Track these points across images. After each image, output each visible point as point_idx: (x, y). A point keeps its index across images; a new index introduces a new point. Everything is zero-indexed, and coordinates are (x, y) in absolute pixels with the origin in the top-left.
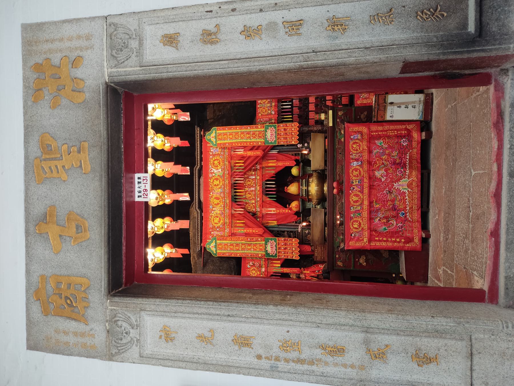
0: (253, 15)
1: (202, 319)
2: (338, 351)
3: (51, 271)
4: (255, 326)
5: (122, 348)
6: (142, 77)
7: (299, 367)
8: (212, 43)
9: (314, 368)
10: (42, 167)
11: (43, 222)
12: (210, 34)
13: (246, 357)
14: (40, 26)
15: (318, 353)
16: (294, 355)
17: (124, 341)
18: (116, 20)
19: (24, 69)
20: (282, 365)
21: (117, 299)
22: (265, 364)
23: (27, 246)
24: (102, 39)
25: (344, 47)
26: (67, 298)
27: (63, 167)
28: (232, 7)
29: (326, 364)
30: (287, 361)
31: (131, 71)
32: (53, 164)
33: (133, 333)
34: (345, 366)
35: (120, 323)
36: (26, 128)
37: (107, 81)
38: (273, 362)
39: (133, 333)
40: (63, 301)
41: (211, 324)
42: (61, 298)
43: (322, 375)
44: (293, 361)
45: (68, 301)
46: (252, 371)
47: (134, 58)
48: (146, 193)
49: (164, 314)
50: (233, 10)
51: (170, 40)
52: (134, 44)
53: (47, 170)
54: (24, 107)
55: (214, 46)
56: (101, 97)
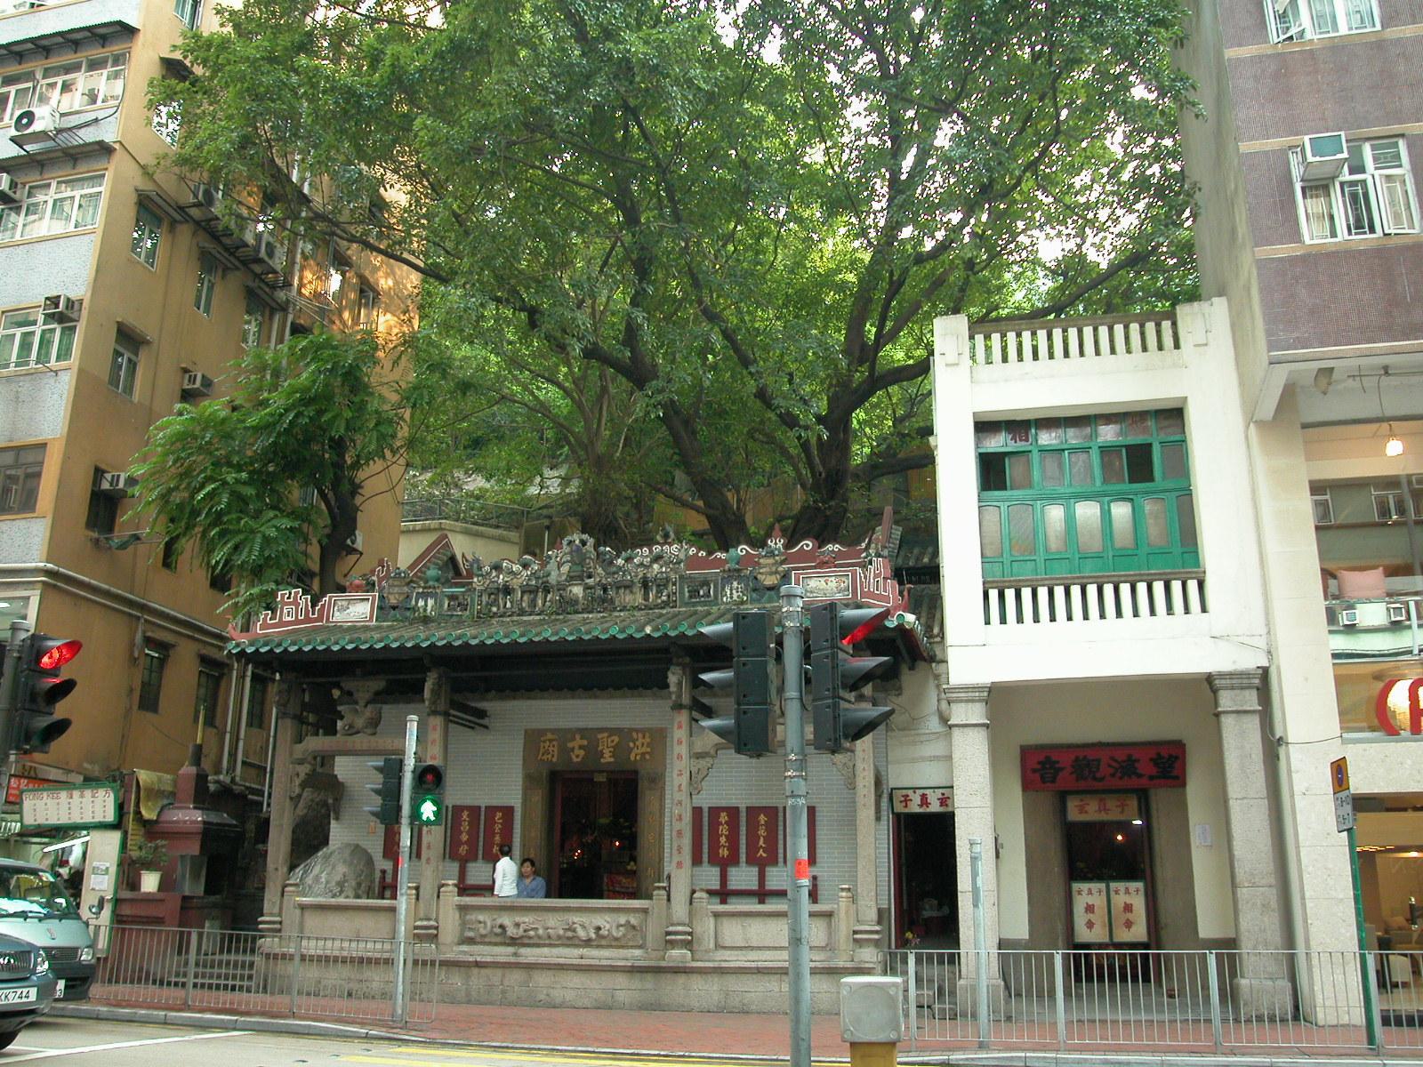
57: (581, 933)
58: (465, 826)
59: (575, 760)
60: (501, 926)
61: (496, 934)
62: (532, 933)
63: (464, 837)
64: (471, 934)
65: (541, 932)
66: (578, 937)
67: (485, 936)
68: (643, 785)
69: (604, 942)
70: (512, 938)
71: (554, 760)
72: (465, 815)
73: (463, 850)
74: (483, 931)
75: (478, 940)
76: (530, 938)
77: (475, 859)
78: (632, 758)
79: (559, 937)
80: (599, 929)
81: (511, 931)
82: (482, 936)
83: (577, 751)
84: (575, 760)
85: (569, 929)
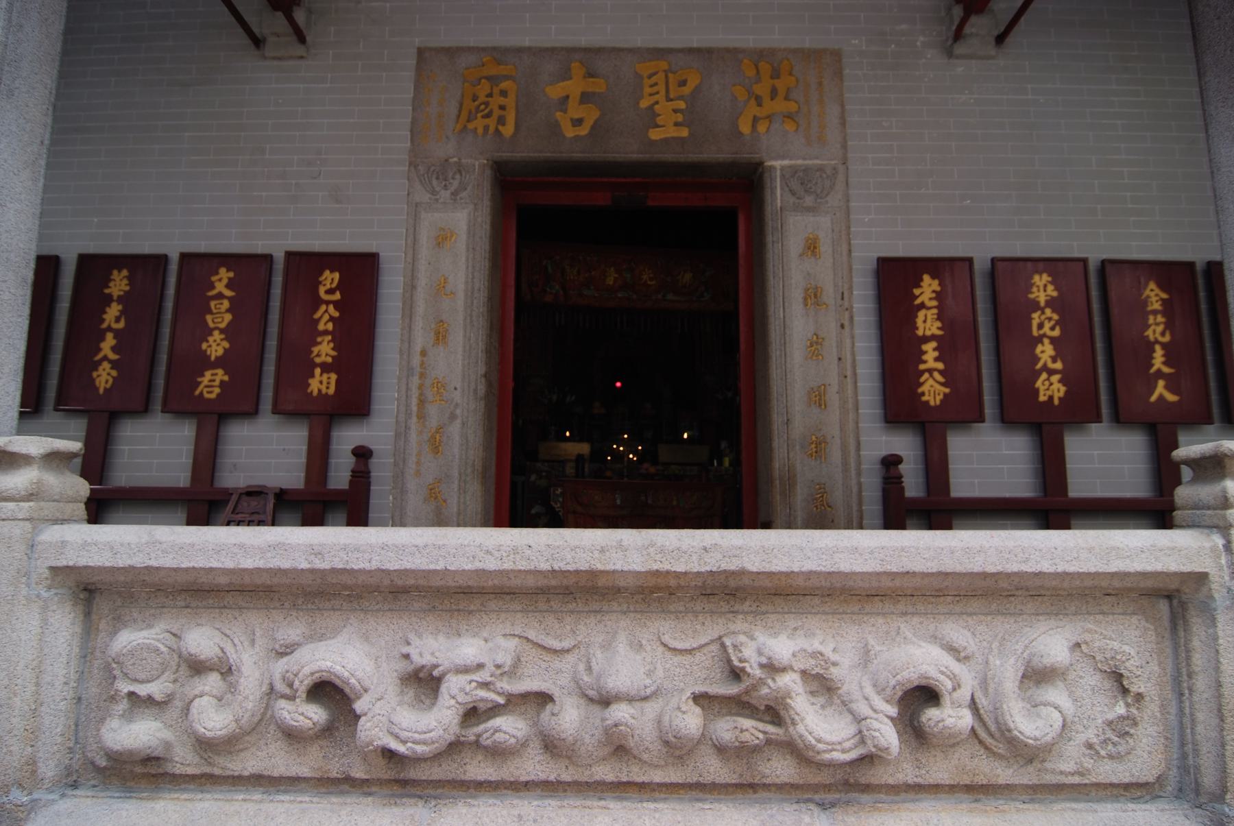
0: (835, 350)
1: (466, 283)
2: (436, 446)
4: (460, 349)
6: (768, 209)
7: (414, 401)
8: (805, 299)
9: (414, 419)
10: (655, 74)
12: (816, 296)
13: (421, 339)
14: (839, 74)
15: (433, 422)
16: (430, 394)
17: (435, 182)
18: (841, 177)
19: (785, 50)
20: (416, 380)
21: (488, 172)
22: (416, 361)
23: (553, 50)
24: (817, 158)
25: (791, 455)
26: (487, 104)
27: (657, 103)
28: (847, 324)
29: (421, 433)
30: (421, 387)
31: (777, 196)
33: (445, 195)
34: (419, 454)
35: (458, 176)
36: (710, 51)
38: (418, 369)
39: (445, 195)
40: (482, 98)
41: (461, 295)
43: (407, 428)
44: (421, 395)
45: (482, 107)
46: (406, 344)
47: (792, 200)
49: (471, 233)
50: (842, 326)
51: (812, 247)
52: (809, 200)
53: (654, 79)
54: (735, 49)
55: (801, 300)
57: (821, 727)
58: (220, 316)
59: (570, 132)
60: (326, 691)
61: (292, 736)
62: (509, 727)
63: (216, 346)
64: (135, 734)
65: (569, 718)
66: (797, 751)
67: (229, 744)
69: (940, 770)
70: (389, 754)
72: (222, 280)
73: (211, 383)
74: (213, 719)
75: (185, 760)
76: (498, 753)
77: (252, 412)
78: (745, 129)
79: (676, 748)
80: (924, 695)
81: (392, 719)
82: (206, 746)
83: (575, 111)
84: (570, 132)
85: (742, 705)
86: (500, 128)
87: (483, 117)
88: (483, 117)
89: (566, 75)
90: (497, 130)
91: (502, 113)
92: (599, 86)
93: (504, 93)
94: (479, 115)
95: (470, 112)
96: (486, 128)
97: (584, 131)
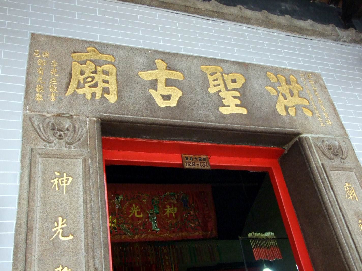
3: (121, 67)
5: (42, 129)
10: (216, 73)
11: (167, 67)
26: (93, 78)
27: (220, 91)
32: (220, 82)
37: (301, 136)
42: (92, 73)
45: (89, 79)
48: (191, 164)
56: (287, 129)
68: (317, 160)
71: (112, 98)
83: (163, 89)
86: (105, 95)
87: (90, 86)
88: (90, 86)
89: (152, 66)
90: (102, 96)
91: (106, 85)
92: (177, 76)
93: (105, 72)
94: (87, 85)
95: (79, 82)
96: (93, 95)
97: (173, 103)
